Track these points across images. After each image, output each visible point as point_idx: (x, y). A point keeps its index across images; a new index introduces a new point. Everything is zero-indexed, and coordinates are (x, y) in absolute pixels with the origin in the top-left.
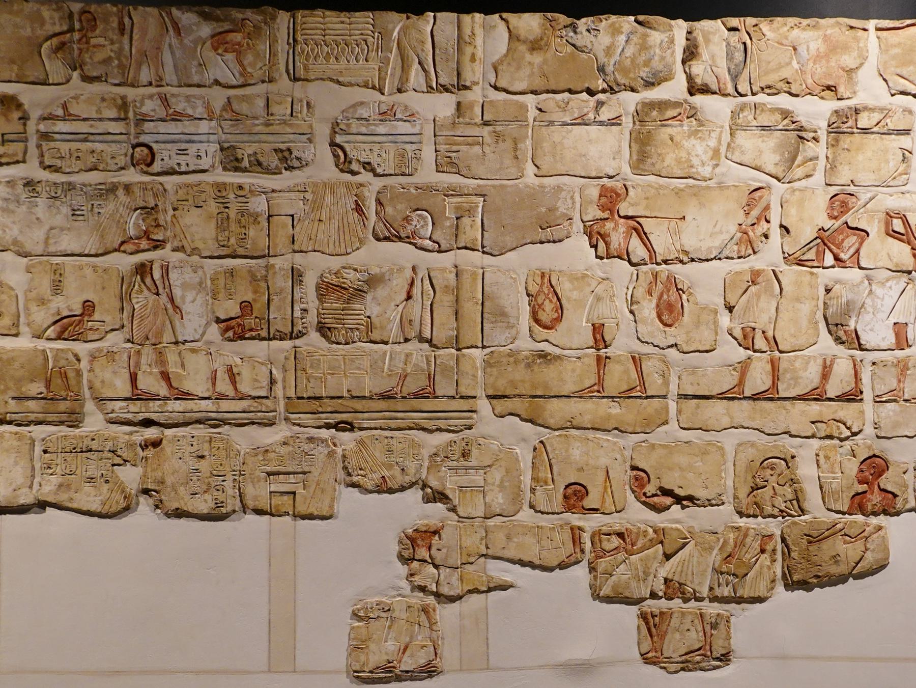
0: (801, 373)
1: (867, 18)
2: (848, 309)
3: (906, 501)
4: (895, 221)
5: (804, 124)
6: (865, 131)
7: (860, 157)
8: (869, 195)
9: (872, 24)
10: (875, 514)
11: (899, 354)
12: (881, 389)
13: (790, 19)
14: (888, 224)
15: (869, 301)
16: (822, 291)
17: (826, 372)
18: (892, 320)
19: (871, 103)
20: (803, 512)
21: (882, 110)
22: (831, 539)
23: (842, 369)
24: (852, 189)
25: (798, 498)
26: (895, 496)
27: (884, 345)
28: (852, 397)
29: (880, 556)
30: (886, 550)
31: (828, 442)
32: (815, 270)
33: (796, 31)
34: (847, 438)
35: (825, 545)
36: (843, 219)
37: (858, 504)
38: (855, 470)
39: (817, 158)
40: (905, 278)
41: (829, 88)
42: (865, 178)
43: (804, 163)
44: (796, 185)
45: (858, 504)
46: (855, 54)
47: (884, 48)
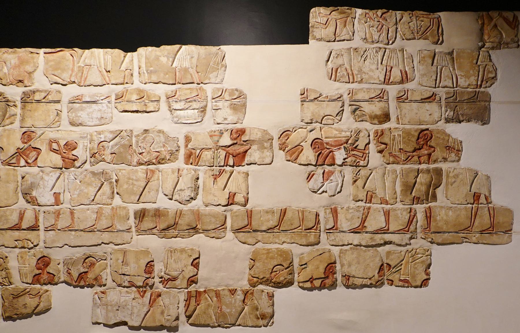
0: (9, 217)
1: (40, 48)
2: (32, 186)
3: (59, 278)
4: (54, 144)
5: (10, 99)
6: (38, 101)
7: (36, 114)
8: (41, 132)
9: (42, 51)
10: (46, 284)
11: (56, 207)
12: (48, 224)
13: (3, 49)
14: (50, 145)
15: (41, 183)
16: (20, 179)
17: (21, 217)
18: (53, 191)
19: (41, 88)
20: (11, 283)
21: (46, 91)
22: (23, 297)
23: (29, 216)
24: (33, 129)
25: (8, 277)
26: (54, 276)
27: (49, 204)
28: (34, 228)
29: (46, 304)
30: (49, 301)
31: (23, 250)
32: (16, 168)
33: (6, 55)
34: (32, 248)
35: (20, 299)
36: (29, 143)
37: (37, 279)
38: (35, 263)
39: (16, 115)
40: (59, 171)
41: (20, 81)
42: (38, 124)
43: (10, 117)
44: (6, 127)
45: (37, 279)
46: (32, 65)
47: (47, 62)
